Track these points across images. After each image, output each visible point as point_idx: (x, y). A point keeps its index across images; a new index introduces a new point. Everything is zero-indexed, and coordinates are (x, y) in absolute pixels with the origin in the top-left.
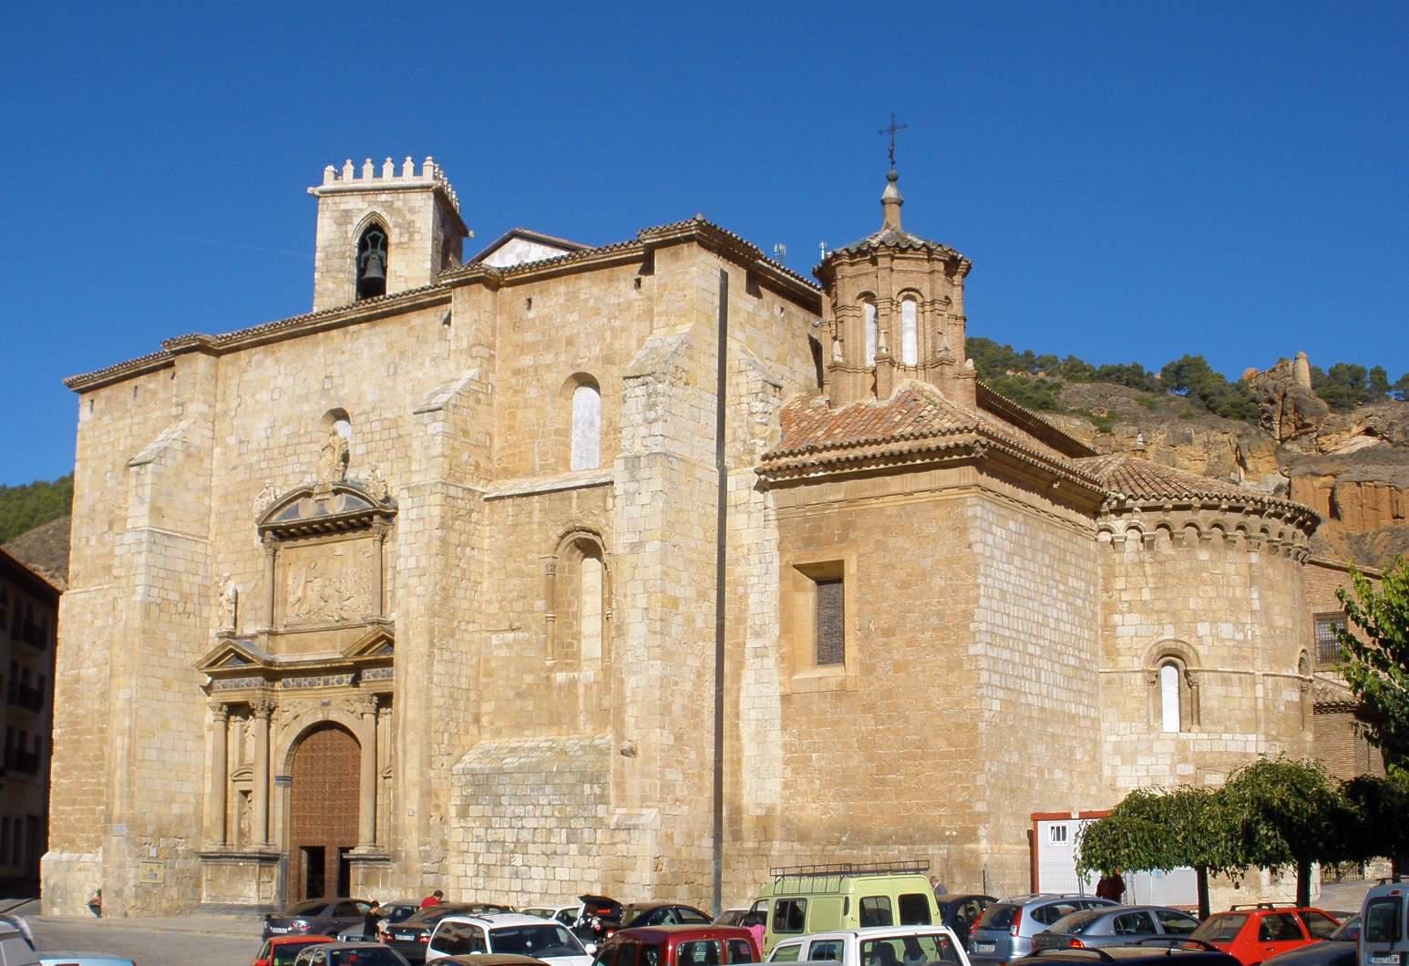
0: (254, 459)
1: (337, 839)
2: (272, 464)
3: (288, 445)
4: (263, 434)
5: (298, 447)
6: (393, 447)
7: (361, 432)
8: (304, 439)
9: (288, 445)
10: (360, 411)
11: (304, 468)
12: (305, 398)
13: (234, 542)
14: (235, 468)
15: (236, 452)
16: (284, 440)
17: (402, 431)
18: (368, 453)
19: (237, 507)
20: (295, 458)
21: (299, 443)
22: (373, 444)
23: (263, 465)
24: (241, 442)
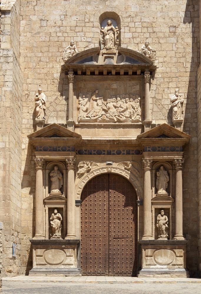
0: (52, 30)
1: (113, 234)
2: (66, 35)
3: (77, 26)
4: (58, 18)
5: (84, 28)
6: (150, 37)
7: (128, 26)
8: (87, 25)
9: (77, 26)
10: (127, 15)
11: (90, 40)
13: (39, 74)
14: (39, 33)
15: (38, 25)
16: (73, 23)
17: (155, 29)
18: (133, 38)
19: (40, 55)
20: (82, 34)
21: (85, 26)
22: (137, 34)
23: (59, 34)
24: (41, 20)
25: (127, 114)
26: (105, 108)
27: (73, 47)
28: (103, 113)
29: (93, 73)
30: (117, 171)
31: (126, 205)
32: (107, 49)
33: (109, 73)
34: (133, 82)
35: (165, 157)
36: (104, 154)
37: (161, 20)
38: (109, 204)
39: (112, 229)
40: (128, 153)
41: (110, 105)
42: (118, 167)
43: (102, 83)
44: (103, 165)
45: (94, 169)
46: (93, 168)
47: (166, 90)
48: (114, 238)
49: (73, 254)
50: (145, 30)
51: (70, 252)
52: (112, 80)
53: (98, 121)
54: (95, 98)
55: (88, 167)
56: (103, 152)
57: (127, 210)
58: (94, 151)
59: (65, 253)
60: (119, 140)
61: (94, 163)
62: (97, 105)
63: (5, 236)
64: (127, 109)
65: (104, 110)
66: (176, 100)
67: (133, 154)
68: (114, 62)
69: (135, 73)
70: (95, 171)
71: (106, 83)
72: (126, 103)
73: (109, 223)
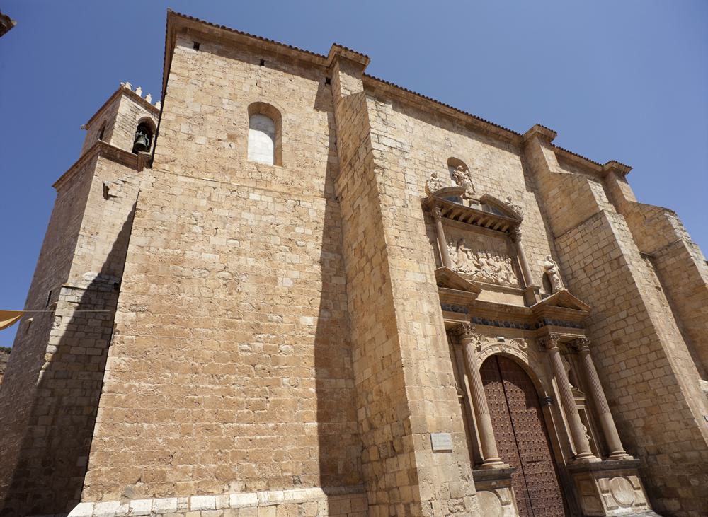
8: (437, 164)
10: (475, 167)
12: (434, 143)
25: (503, 273)
26: (476, 263)
27: (437, 179)
28: (476, 269)
29: (456, 218)
30: (513, 352)
31: (528, 406)
32: (470, 194)
33: (475, 222)
34: (497, 239)
35: (570, 335)
36: (492, 325)
37: (505, 182)
38: (507, 402)
39: (521, 446)
40: (518, 328)
41: (483, 260)
42: (511, 345)
43: (465, 232)
44: (493, 341)
45: (485, 346)
46: (484, 345)
47: (532, 255)
48: (528, 462)
49: (510, 499)
50: (495, 187)
51: (506, 494)
52: (477, 232)
53: (474, 278)
54: (463, 249)
55: (477, 341)
56: (490, 323)
57: (531, 413)
58: (479, 319)
59: (499, 497)
60: (512, 306)
61: (483, 337)
62: (468, 257)
63: (460, 466)
64: (500, 269)
65: (476, 265)
66: (553, 266)
67: (522, 328)
68: (480, 207)
69: (499, 229)
70: (488, 348)
71: (471, 234)
72: (498, 262)
73: (515, 436)
